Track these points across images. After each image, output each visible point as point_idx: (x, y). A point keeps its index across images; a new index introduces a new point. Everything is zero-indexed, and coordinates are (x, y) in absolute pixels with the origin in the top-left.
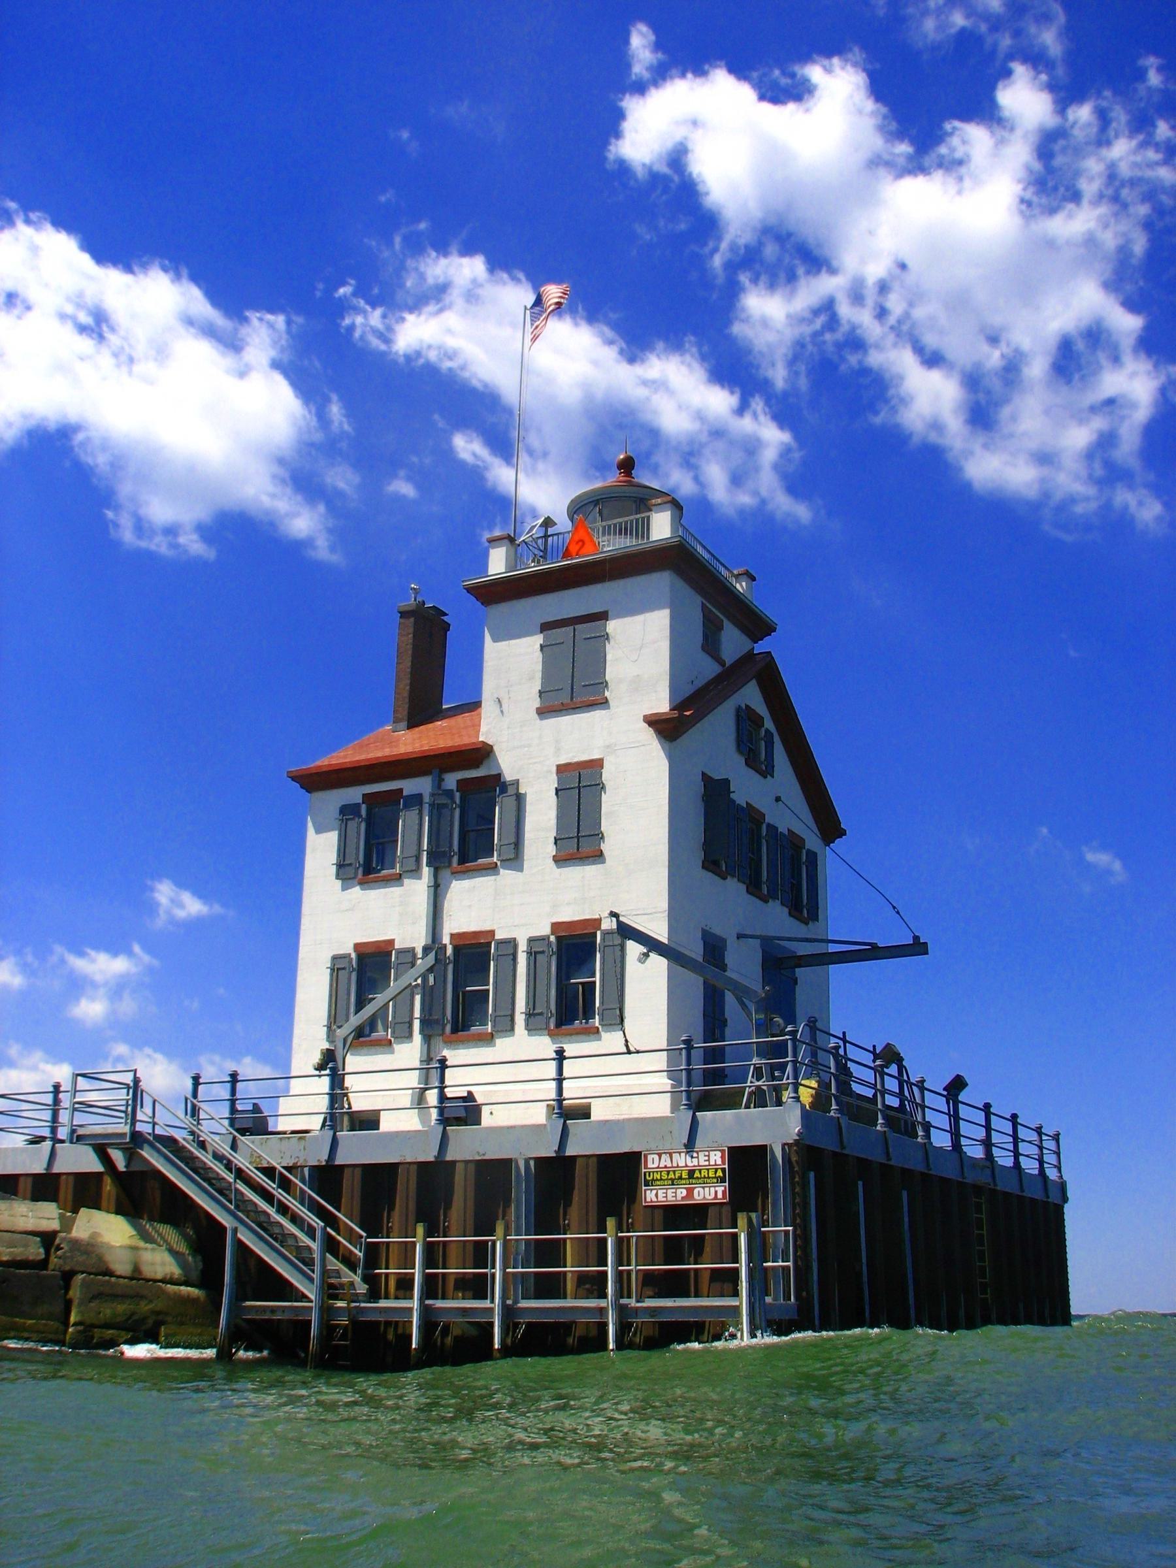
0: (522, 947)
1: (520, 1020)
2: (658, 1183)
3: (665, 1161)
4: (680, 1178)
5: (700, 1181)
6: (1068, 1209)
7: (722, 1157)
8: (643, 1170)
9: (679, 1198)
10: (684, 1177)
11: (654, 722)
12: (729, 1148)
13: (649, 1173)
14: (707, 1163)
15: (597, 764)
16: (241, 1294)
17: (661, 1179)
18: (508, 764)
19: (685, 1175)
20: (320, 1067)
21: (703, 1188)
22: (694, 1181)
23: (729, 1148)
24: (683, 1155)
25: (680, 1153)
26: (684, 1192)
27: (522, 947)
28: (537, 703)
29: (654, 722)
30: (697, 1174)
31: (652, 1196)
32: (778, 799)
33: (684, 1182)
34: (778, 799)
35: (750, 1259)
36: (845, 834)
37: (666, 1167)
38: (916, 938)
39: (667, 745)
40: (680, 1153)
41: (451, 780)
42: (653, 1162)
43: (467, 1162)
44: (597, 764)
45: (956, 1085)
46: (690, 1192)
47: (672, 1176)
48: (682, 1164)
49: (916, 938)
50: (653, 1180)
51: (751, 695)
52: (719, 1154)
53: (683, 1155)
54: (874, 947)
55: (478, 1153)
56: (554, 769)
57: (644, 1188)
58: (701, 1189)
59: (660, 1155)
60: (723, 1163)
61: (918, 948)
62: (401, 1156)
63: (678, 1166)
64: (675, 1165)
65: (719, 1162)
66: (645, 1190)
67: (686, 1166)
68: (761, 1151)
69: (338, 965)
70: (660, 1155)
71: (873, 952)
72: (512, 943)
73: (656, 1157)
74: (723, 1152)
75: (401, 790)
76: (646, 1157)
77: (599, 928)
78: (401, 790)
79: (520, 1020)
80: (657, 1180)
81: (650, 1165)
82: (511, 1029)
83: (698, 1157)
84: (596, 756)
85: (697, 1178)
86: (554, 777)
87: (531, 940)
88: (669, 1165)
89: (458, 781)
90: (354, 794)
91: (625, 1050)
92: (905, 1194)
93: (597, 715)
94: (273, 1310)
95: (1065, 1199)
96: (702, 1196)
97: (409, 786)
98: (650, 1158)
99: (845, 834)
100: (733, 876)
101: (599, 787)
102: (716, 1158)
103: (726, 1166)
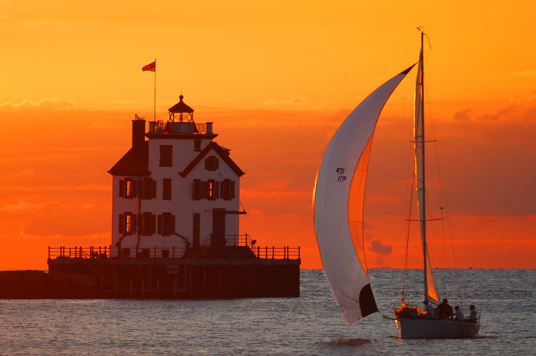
0: (157, 217)
1: (156, 232)
11: (180, 173)
18: (153, 177)
20: (116, 246)
27: (157, 217)
28: (159, 164)
31: (168, 272)
38: (244, 211)
41: (142, 178)
49: (244, 211)
75: (132, 179)
78: (132, 179)
79: (156, 232)
87: (159, 216)
89: (144, 178)
93: (170, 168)
100: (203, 198)
102: (177, 267)
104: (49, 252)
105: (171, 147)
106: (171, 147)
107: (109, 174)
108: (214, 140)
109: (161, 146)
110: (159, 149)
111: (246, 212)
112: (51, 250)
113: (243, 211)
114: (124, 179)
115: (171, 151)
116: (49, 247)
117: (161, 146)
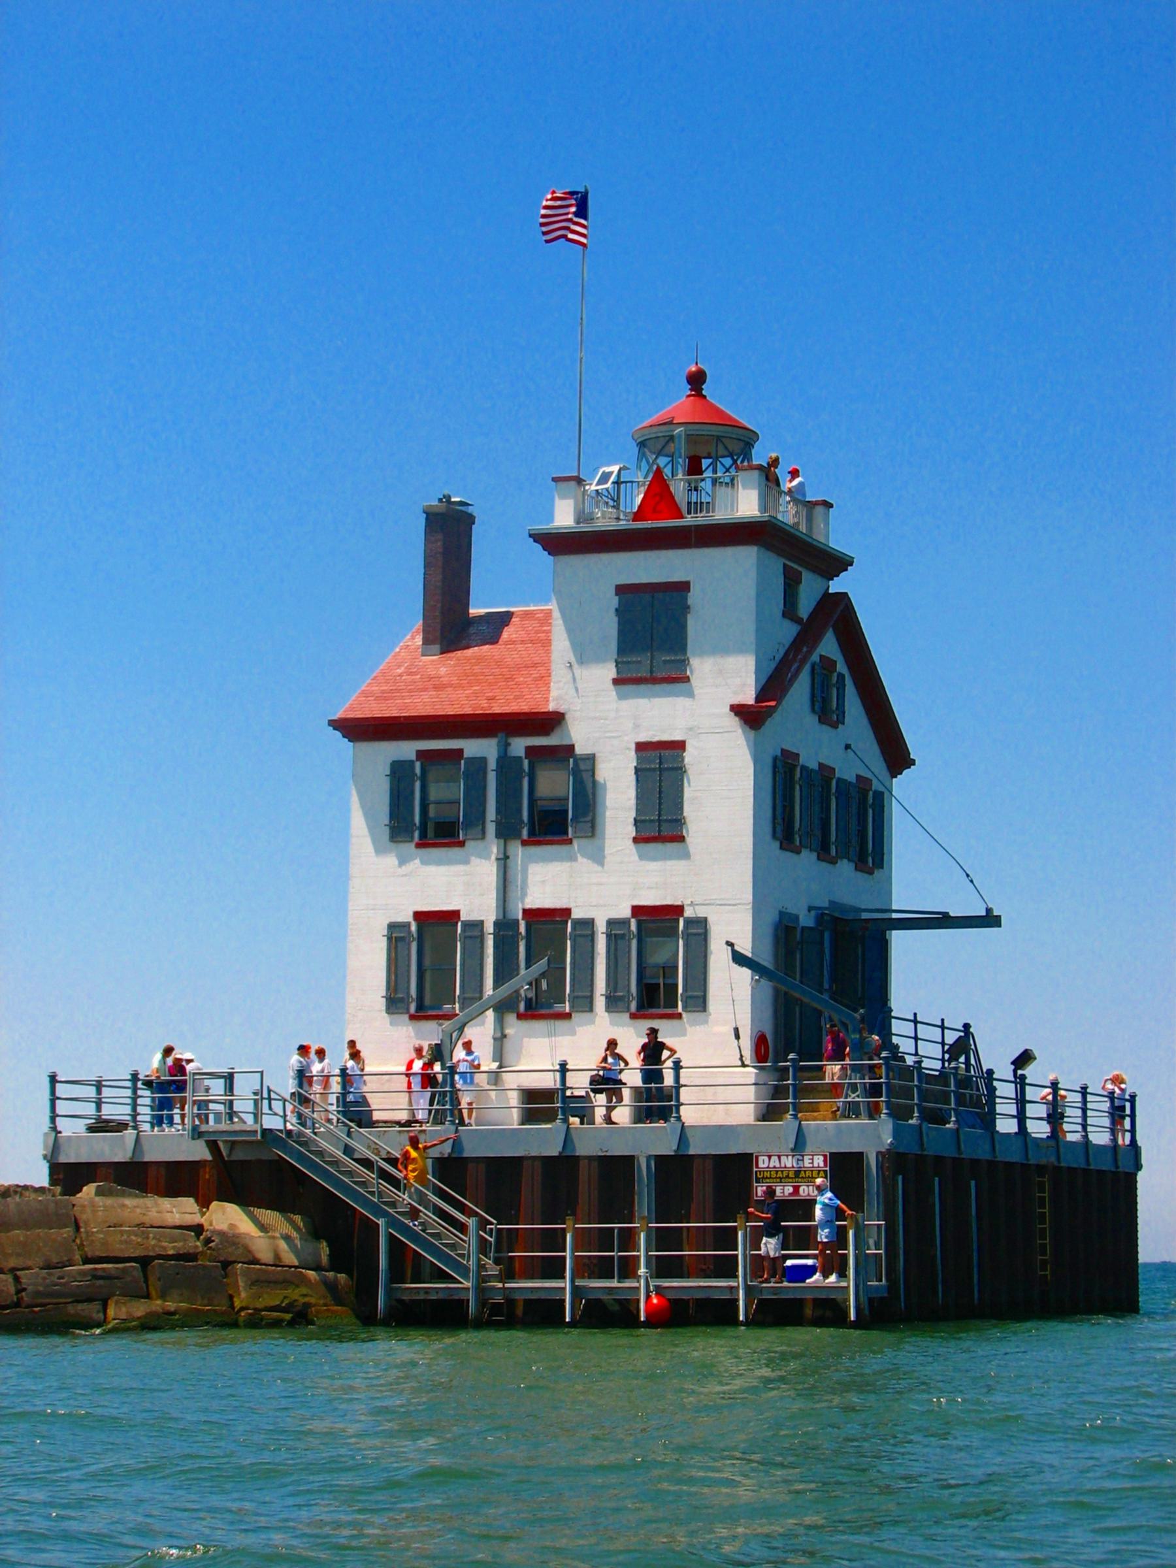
0: (601, 927)
1: (600, 1002)
2: (768, 1180)
3: (774, 1162)
4: (788, 1177)
5: (805, 1180)
6: (1141, 1176)
7: (825, 1161)
8: (755, 1169)
9: (786, 1194)
10: (790, 1176)
11: (738, 710)
12: (830, 1153)
13: (760, 1171)
14: (811, 1165)
15: (680, 746)
16: (396, 1275)
17: (770, 1178)
19: (791, 1175)
21: (808, 1186)
22: (800, 1180)
23: (830, 1153)
24: (790, 1157)
25: (787, 1156)
26: (791, 1190)
27: (601, 927)
29: (738, 710)
30: (802, 1174)
32: (848, 747)
33: (791, 1180)
34: (848, 747)
35: (856, 1248)
36: (914, 764)
37: (775, 1167)
38: (989, 910)
39: (752, 733)
40: (787, 1156)
41: (519, 746)
42: (763, 1163)
43: (590, 1158)
44: (680, 746)
45: (1024, 1059)
46: (796, 1190)
47: (780, 1175)
48: (789, 1165)
49: (989, 910)
50: (763, 1178)
51: (829, 646)
52: (822, 1158)
53: (790, 1157)
54: (945, 915)
55: (601, 1149)
56: (633, 746)
57: (755, 1184)
58: (806, 1188)
59: (770, 1157)
60: (825, 1165)
61: (990, 920)
62: (525, 1150)
63: (785, 1167)
64: (783, 1165)
65: (822, 1164)
66: (757, 1187)
67: (793, 1167)
68: (857, 1158)
69: (396, 935)
70: (770, 1157)
71: (943, 921)
72: (589, 923)
73: (766, 1159)
74: (825, 1156)
75: (461, 751)
76: (757, 1158)
77: (682, 916)
78: (460, 752)
79: (600, 1002)
80: (767, 1178)
81: (761, 1165)
82: (590, 1008)
83: (803, 1160)
84: (677, 737)
85: (802, 1178)
86: (632, 754)
87: (611, 923)
88: (778, 1165)
90: (407, 749)
91: (739, 1063)
92: (973, 1183)
94: (427, 1290)
95: (1138, 1167)
96: (806, 1193)
97: (472, 747)
98: (761, 1159)
99: (914, 764)
101: (679, 771)
102: (819, 1161)
103: (828, 1169)
104: (54, 1099)
105: (684, 587)
106: (684, 587)
107: (338, 734)
108: (836, 586)
109: (621, 590)
110: (615, 601)
111: (999, 917)
112: (61, 1090)
113: (984, 913)
114: (413, 757)
115: (686, 608)
116: (53, 1079)
117: (621, 590)
